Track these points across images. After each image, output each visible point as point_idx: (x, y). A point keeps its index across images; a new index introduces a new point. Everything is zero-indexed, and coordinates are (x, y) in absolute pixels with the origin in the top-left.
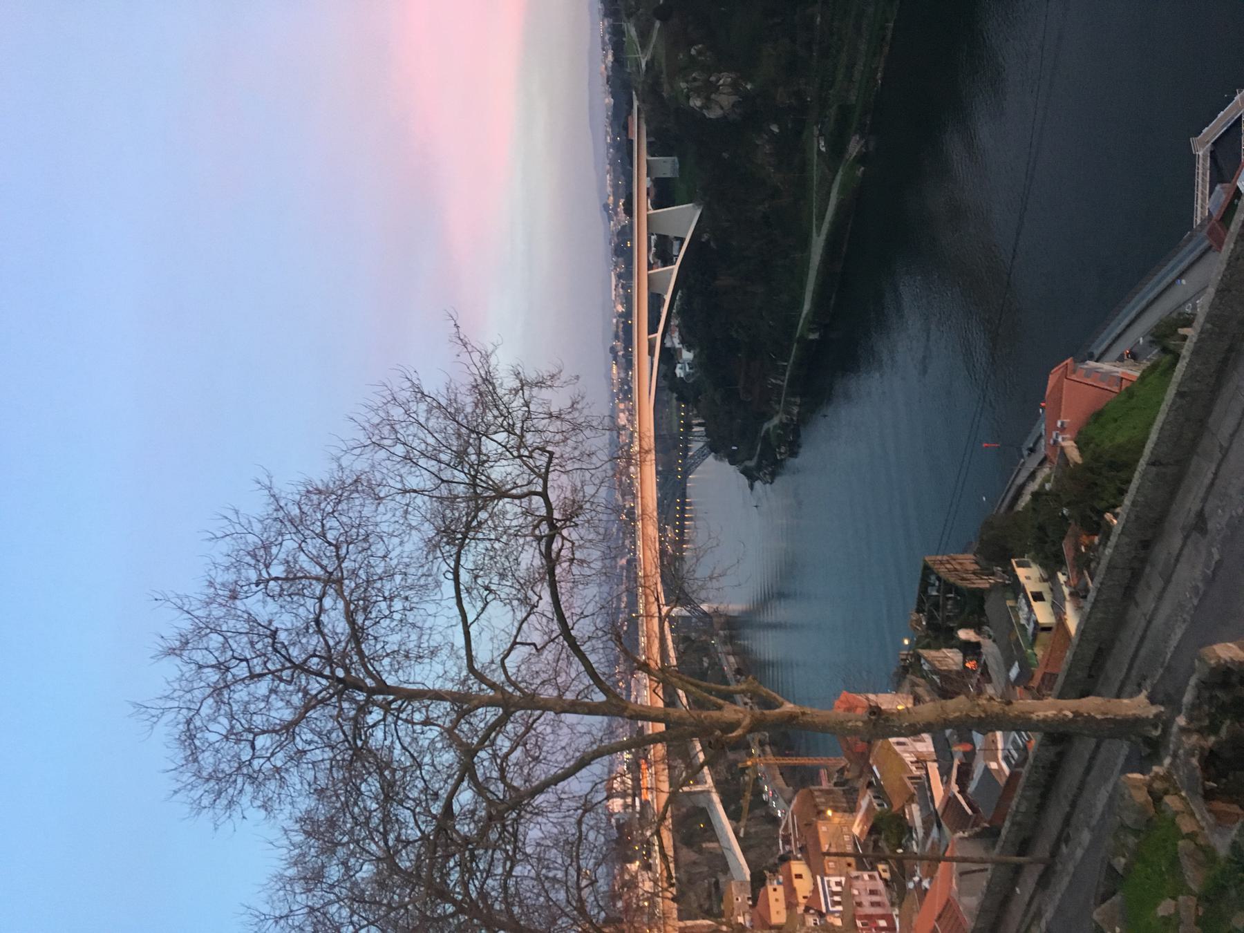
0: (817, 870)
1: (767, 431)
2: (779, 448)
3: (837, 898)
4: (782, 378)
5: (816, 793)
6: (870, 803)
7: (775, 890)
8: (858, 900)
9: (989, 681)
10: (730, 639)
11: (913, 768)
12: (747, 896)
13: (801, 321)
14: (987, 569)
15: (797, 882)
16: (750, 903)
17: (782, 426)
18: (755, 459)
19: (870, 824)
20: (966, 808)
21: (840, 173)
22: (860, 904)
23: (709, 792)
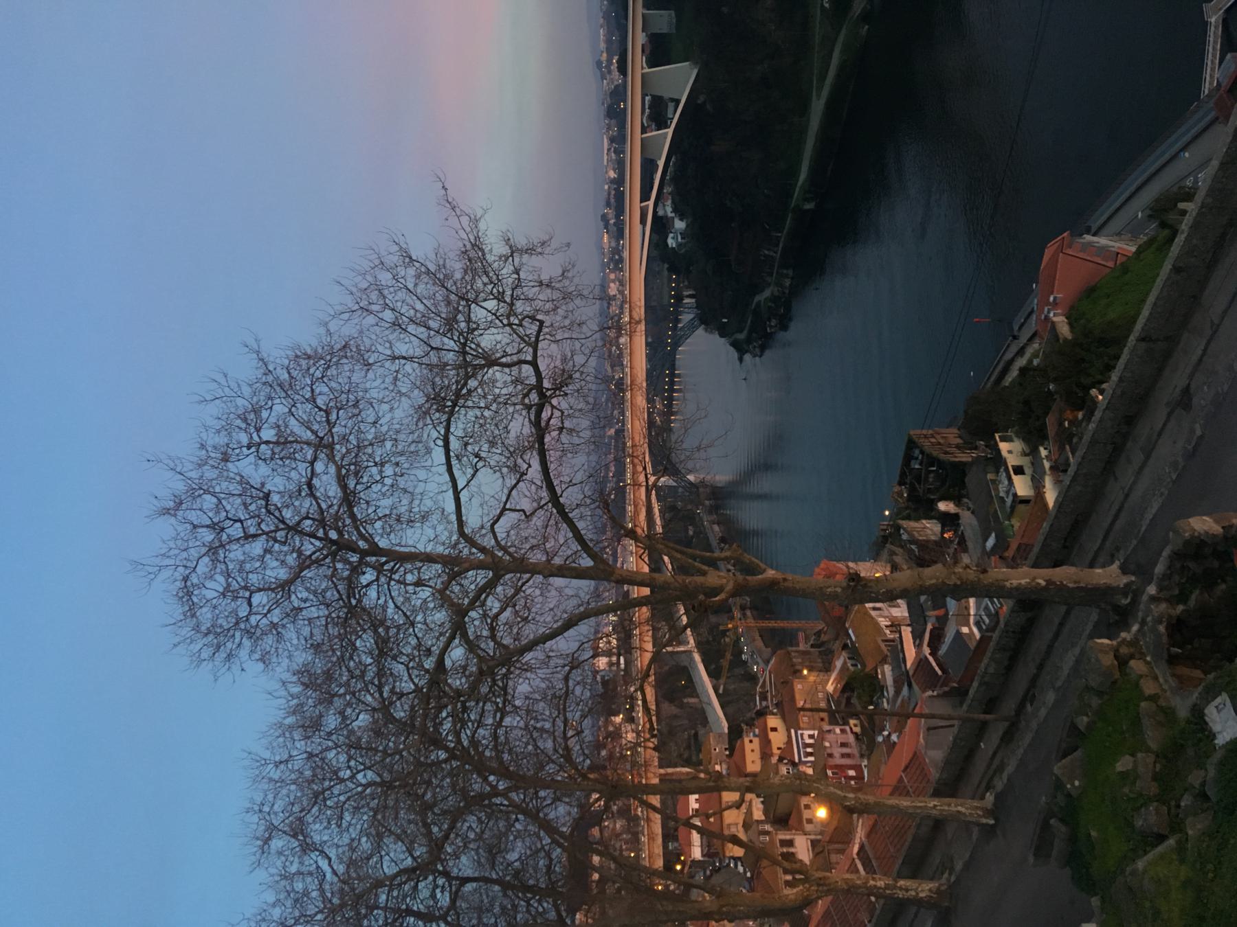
0: (791, 723)
1: (759, 303)
2: (769, 320)
3: (809, 750)
4: (776, 249)
5: (793, 654)
6: (845, 663)
7: (751, 741)
8: (829, 751)
9: (966, 550)
10: (714, 509)
11: (888, 632)
12: (724, 747)
13: (797, 189)
14: (971, 443)
15: (772, 735)
16: (727, 753)
17: (774, 299)
18: (745, 332)
19: (843, 683)
20: (937, 668)
21: (844, 32)
22: (830, 755)
23: (690, 652)
